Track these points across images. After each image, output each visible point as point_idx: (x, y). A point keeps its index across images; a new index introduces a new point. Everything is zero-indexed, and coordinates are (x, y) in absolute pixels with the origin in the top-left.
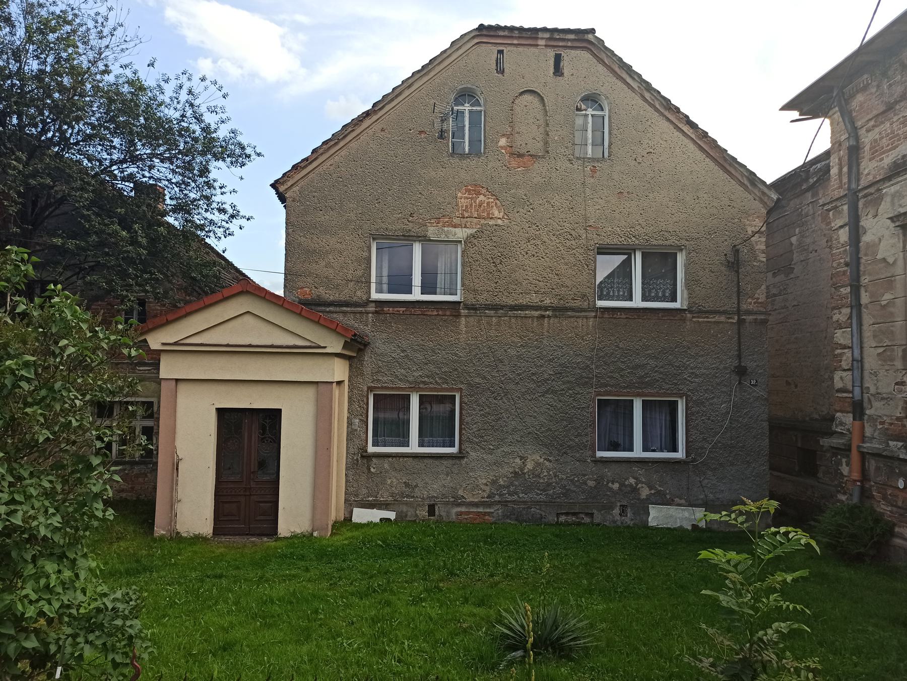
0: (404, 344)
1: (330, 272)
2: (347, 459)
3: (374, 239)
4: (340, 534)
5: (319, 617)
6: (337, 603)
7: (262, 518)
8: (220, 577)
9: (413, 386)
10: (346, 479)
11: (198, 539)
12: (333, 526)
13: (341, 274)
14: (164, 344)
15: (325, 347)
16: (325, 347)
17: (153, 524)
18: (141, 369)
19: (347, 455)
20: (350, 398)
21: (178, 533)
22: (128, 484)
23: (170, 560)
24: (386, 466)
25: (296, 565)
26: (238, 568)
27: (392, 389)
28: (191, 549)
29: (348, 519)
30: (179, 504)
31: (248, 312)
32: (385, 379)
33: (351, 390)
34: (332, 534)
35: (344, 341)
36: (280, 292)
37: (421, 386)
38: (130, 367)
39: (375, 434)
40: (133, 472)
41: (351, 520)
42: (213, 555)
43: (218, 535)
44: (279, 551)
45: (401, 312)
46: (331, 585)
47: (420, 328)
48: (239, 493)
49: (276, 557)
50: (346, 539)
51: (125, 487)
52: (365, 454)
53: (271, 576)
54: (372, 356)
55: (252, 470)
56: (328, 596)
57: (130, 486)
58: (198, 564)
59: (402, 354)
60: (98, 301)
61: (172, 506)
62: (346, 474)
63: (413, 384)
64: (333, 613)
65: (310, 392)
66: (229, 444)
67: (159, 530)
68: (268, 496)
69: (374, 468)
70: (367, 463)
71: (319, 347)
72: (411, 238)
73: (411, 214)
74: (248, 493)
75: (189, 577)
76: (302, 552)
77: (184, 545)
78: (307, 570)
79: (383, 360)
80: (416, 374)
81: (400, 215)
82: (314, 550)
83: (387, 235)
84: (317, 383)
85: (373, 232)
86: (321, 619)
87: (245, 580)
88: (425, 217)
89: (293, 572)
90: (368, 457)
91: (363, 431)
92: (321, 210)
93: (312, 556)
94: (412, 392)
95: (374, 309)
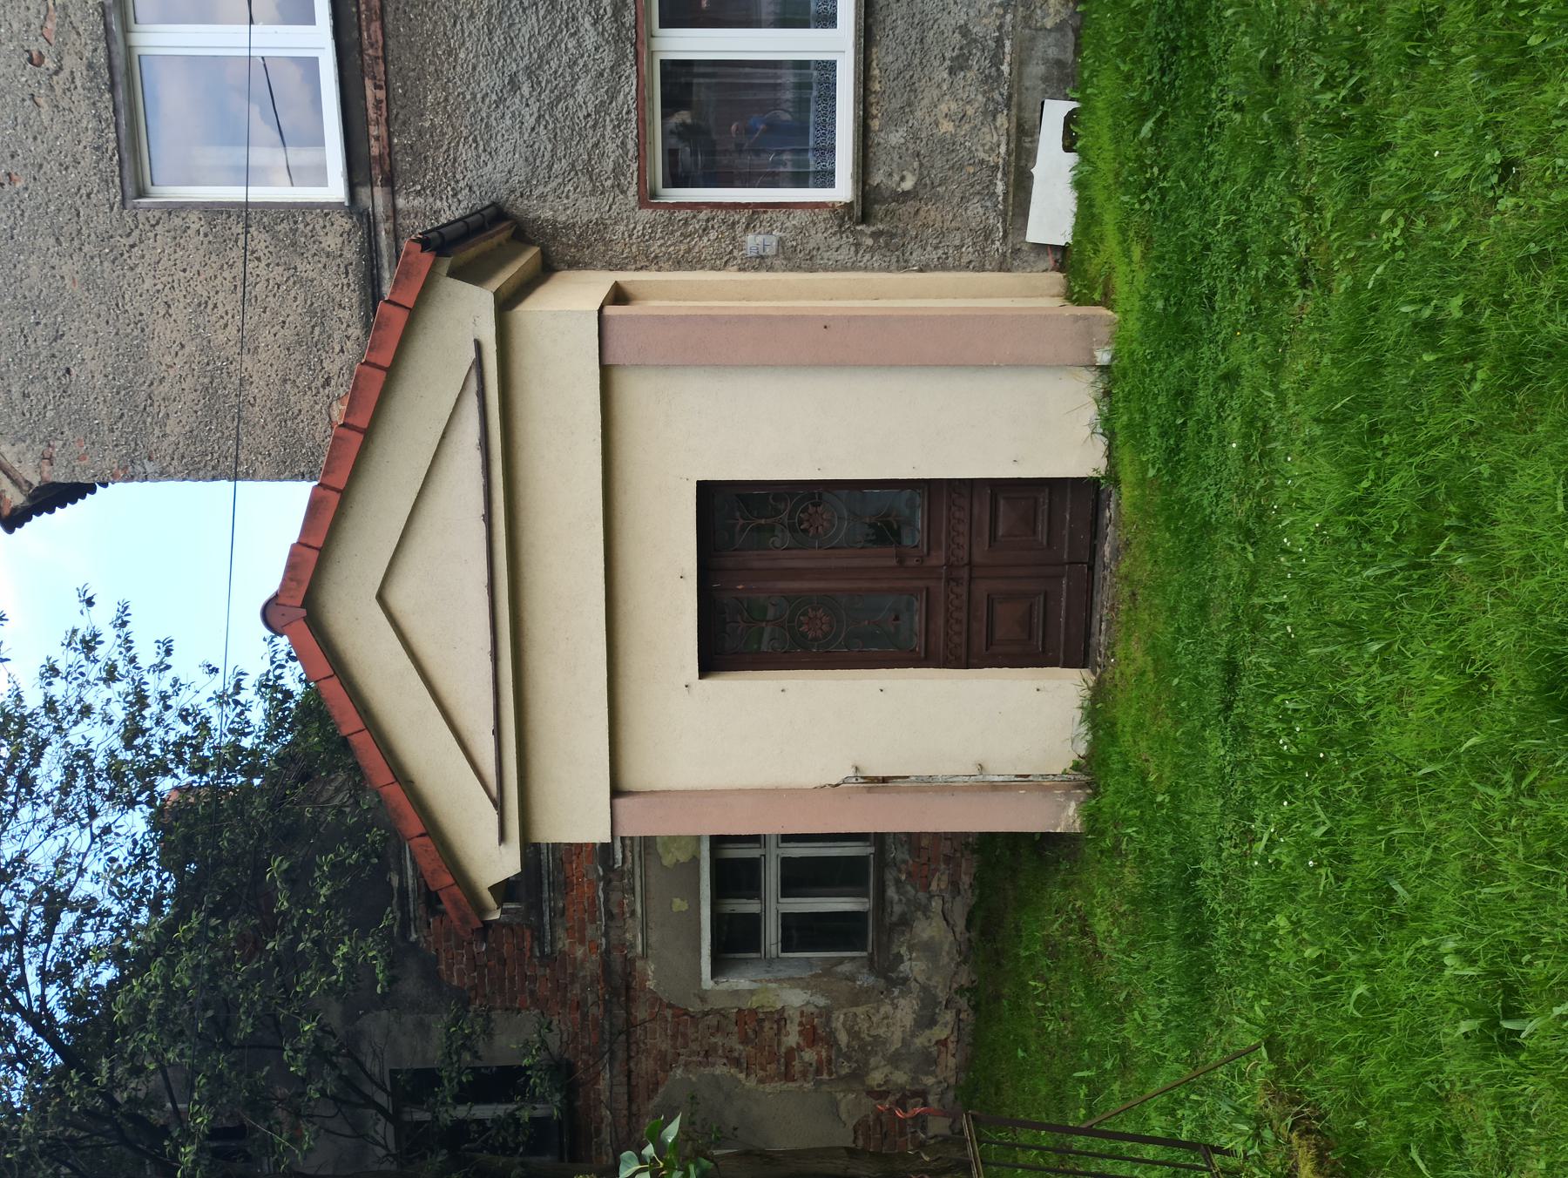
0: (490, 81)
1: (270, 338)
2: (873, 270)
3: (142, 193)
4: (1108, 278)
5: (1457, 314)
6: (1394, 249)
7: (1042, 527)
8: (1232, 670)
9: (630, 50)
10: (936, 269)
11: (1098, 713)
12: (1079, 302)
13: (272, 302)
14: (503, 838)
15: (478, 346)
16: (478, 346)
17: (1047, 837)
18: (619, 856)
19: (859, 269)
20: (679, 264)
21: (1076, 767)
22: (936, 870)
23: (1161, 805)
24: (896, 137)
25: (1208, 417)
26: (1203, 607)
27: (643, 123)
28: (1128, 737)
29: (1062, 258)
30: (990, 767)
31: (381, 598)
32: (611, 147)
33: (652, 262)
34: (1107, 301)
35: (450, 280)
36: (299, 493)
37: (629, 19)
38: (615, 883)
39: (800, 180)
40: (905, 862)
41: (1063, 250)
42: (1152, 675)
43: (1086, 654)
44: (1151, 473)
45: (381, 94)
46: (1304, 282)
47: (429, 26)
48: (965, 597)
49: (1175, 482)
50: (1127, 253)
51: (945, 878)
52: (857, 211)
53: (1241, 502)
54: (536, 193)
55: (894, 562)
56: (1354, 291)
57: (943, 866)
58: (1177, 723)
59: (526, 89)
60: (438, 972)
61: (994, 787)
62: (921, 270)
63: (623, 50)
64: (1443, 254)
65: (636, 391)
66: (811, 635)
67: (1066, 817)
68: (976, 511)
69: (903, 179)
70: (884, 201)
71: (479, 363)
72: (119, 62)
73: (35, 60)
74: (965, 573)
75: (1222, 769)
76: (1161, 400)
77: (1115, 757)
78: (1231, 378)
79: (548, 155)
80: (590, 39)
81: (41, 101)
82: (1156, 357)
83: (118, 147)
84: (605, 371)
85: (114, 193)
86: (1468, 306)
87: (1250, 588)
88: (33, 11)
89: (1235, 427)
90: (868, 203)
91: (783, 217)
92: (68, 371)
93: (1179, 363)
94: (651, 54)
95: (379, 192)
